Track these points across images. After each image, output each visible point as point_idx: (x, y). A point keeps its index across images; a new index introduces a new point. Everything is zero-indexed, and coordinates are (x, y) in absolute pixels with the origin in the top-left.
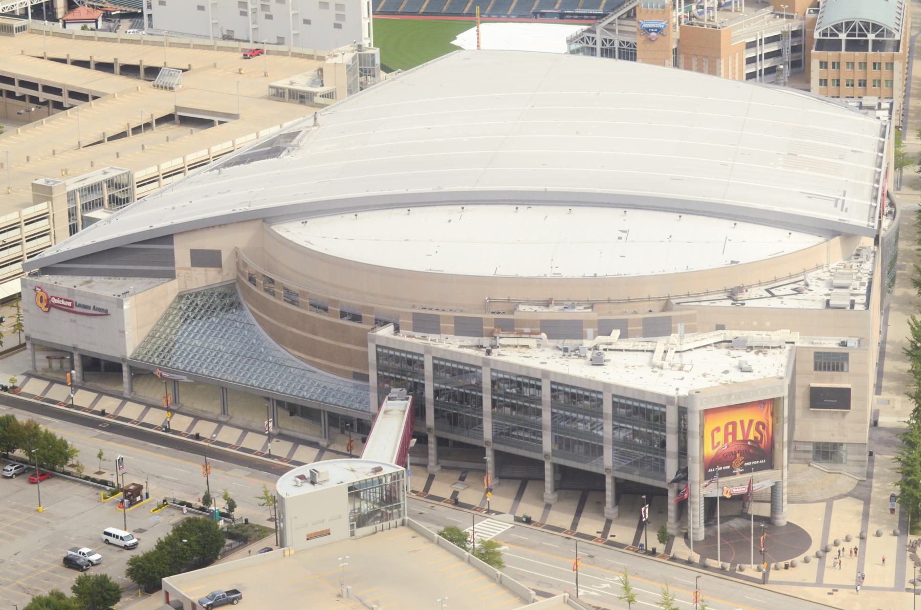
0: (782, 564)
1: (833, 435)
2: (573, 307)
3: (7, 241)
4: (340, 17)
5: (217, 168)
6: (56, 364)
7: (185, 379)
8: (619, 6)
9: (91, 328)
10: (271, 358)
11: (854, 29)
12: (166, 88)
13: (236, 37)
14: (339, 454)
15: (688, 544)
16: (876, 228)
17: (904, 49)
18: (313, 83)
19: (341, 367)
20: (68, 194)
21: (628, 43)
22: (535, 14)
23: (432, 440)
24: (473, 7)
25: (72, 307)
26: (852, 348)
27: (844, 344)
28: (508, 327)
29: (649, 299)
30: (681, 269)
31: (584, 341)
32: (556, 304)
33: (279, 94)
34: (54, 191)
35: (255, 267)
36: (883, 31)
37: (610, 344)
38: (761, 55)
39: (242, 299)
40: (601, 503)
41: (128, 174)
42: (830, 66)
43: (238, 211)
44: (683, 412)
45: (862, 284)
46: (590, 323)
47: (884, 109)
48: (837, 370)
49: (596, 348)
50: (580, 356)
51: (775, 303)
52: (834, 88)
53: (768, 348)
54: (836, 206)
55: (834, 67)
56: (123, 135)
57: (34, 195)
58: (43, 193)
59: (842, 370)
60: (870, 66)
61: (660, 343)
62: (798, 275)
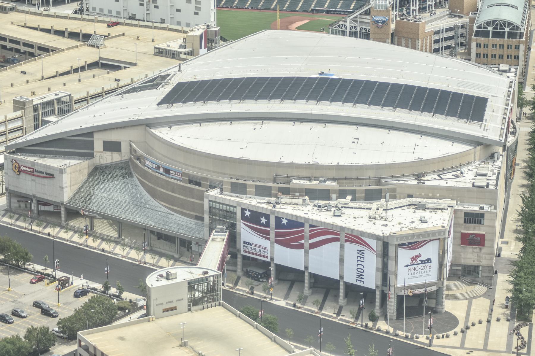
0: (441, 335)
1: (474, 261)
2: (325, 181)
4: (197, 8)
5: (121, 94)
6: (23, 205)
8: (361, 7)
9: (44, 185)
10: (148, 206)
11: (497, 25)
12: (94, 46)
14: (185, 263)
16: (503, 141)
17: (526, 38)
18: (181, 47)
19: (188, 212)
21: (365, 29)
22: (313, 10)
24: (276, 5)
25: (33, 172)
26: (487, 212)
27: (481, 208)
28: (286, 192)
29: (369, 178)
30: (389, 161)
31: (331, 202)
32: (315, 180)
33: (160, 52)
34: (26, 104)
35: (140, 152)
36: (514, 27)
37: (346, 204)
38: (442, 38)
39: (132, 170)
40: (337, 296)
41: (70, 95)
42: (482, 46)
43: (131, 119)
45: (494, 174)
46: (334, 192)
47: (512, 72)
48: (478, 223)
50: (328, 211)
51: (442, 183)
52: (483, 59)
53: (438, 209)
54: (481, 127)
55: (484, 47)
56: (68, 73)
57: (14, 106)
58: (19, 105)
59: (480, 223)
60: (506, 47)
61: (375, 205)
62: (457, 167)
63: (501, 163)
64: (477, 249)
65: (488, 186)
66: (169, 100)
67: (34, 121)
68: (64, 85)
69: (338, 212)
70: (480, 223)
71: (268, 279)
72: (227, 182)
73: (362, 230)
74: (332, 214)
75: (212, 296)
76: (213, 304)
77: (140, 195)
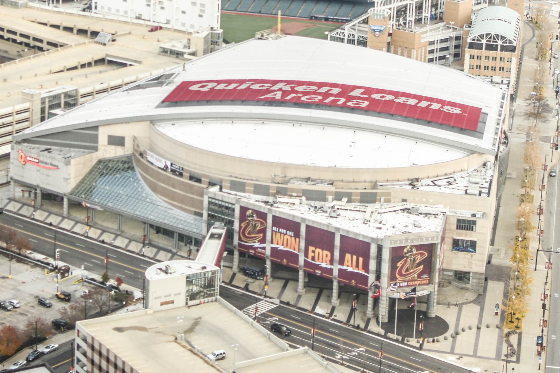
3: (5, 123)
5: (126, 90)
7: (99, 208)
12: (102, 44)
13: (143, 18)
15: (378, 322)
16: (496, 151)
19: (187, 208)
20: (42, 99)
23: (236, 253)
30: (384, 166)
31: (326, 203)
37: (341, 206)
39: (134, 165)
41: (76, 90)
44: (380, 249)
46: (331, 193)
48: (470, 230)
49: (333, 207)
50: (324, 212)
56: (75, 68)
61: (370, 207)
62: (450, 174)
63: (492, 172)
64: (468, 255)
65: (480, 194)
66: (174, 99)
67: (41, 114)
68: (72, 79)
69: (334, 213)
70: (472, 230)
71: (263, 277)
72: (227, 180)
73: (357, 232)
74: (327, 215)
75: (210, 291)
76: (210, 299)
77: (141, 189)
